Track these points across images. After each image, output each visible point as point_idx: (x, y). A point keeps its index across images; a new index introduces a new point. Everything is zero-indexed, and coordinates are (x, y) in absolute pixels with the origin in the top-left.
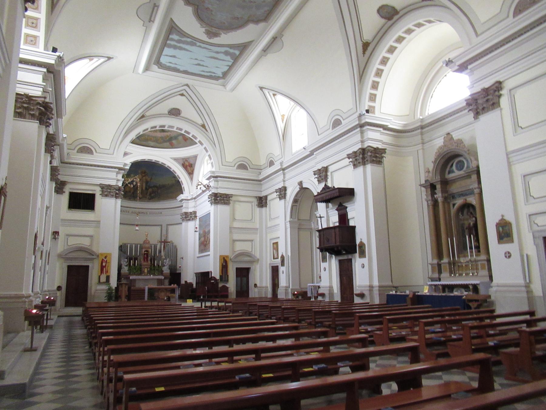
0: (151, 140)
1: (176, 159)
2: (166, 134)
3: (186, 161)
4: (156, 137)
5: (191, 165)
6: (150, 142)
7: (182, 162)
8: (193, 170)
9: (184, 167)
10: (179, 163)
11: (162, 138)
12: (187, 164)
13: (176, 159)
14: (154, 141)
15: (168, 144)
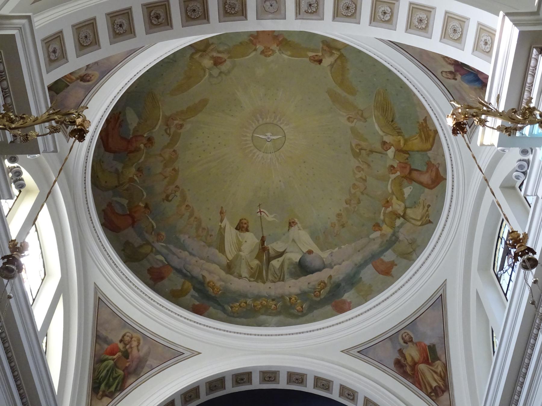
0: (266, 310)
1: (365, 352)
2: (314, 278)
3: (408, 341)
4: (282, 297)
5: (432, 348)
6: (263, 318)
7: (390, 354)
8: (446, 367)
9: (405, 374)
10: (380, 363)
11: (303, 295)
12: (413, 353)
13: (365, 352)
14: (278, 313)
15: (329, 308)
